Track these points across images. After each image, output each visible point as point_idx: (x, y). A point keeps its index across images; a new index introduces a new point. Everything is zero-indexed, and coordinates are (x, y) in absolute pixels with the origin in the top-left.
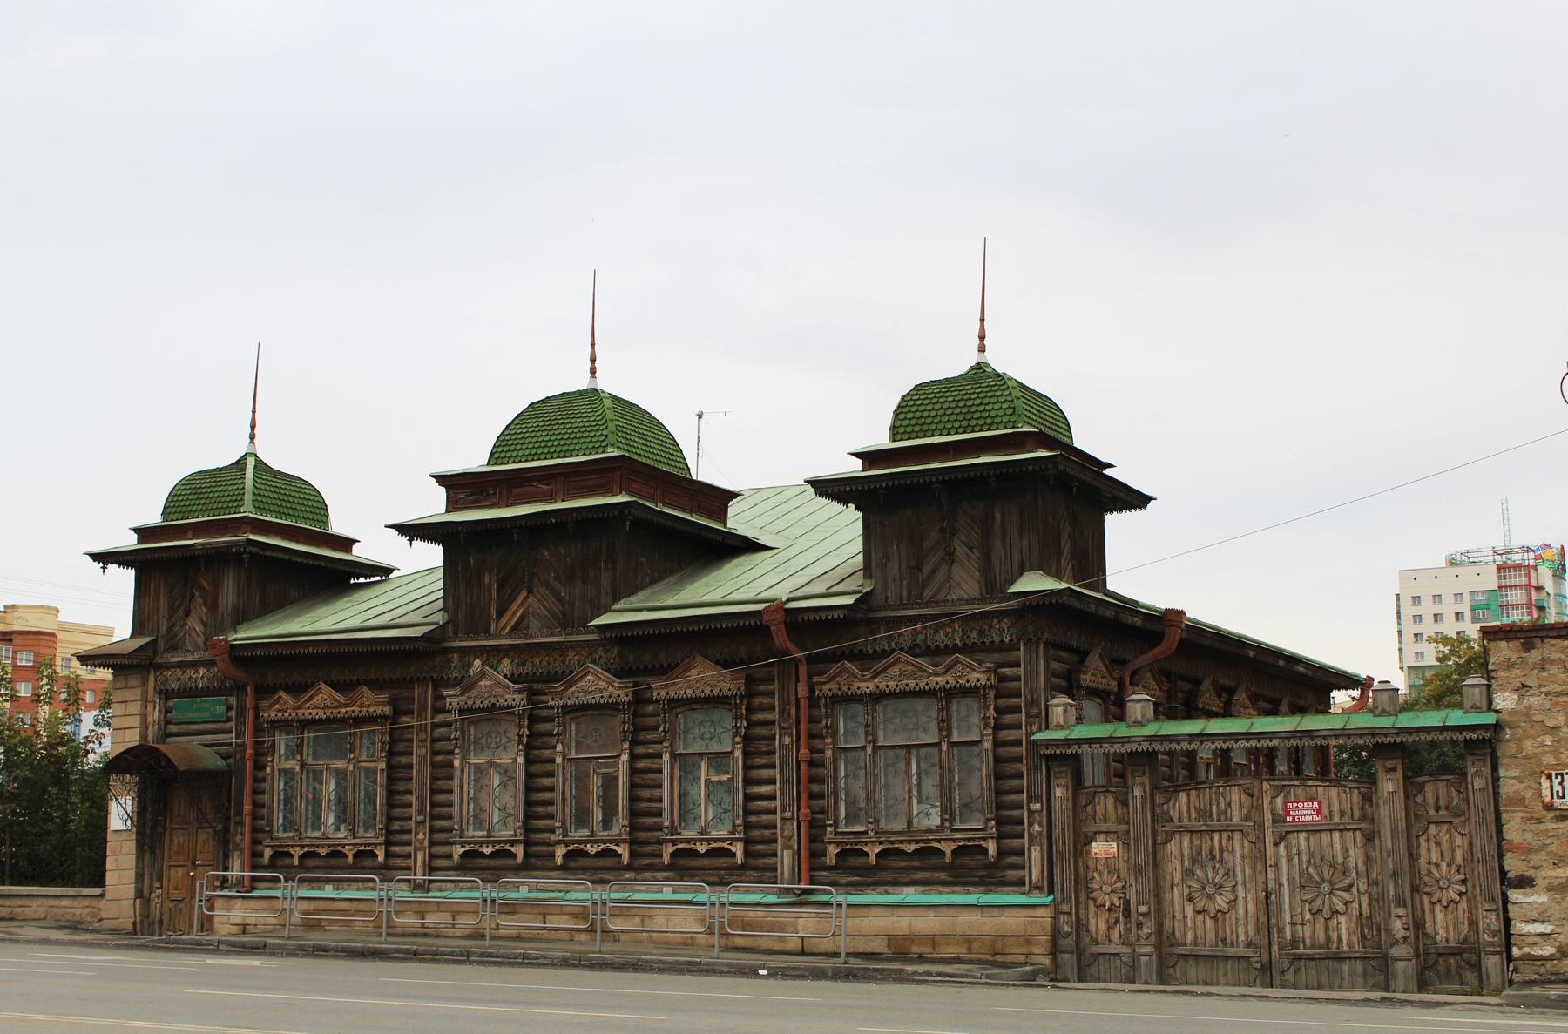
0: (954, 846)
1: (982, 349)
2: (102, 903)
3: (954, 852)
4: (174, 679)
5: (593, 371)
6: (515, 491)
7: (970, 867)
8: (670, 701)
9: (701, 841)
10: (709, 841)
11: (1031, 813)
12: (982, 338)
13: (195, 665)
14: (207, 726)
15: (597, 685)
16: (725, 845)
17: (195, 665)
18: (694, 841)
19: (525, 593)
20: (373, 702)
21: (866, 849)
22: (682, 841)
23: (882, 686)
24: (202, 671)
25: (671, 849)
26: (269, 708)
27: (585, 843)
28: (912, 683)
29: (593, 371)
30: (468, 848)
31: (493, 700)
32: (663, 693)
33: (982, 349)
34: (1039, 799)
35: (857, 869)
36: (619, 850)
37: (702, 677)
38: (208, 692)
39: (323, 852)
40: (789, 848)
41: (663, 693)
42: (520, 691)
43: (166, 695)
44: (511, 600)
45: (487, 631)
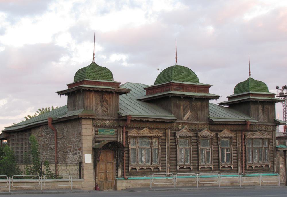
0: (265, 165)
1: (250, 75)
2: (83, 183)
3: (265, 167)
4: (99, 123)
5: (176, 61)
6: (187, 89)
7: (267, 170)
8: (221, 137)
9: (226, 165)
10: (227, 165)
11: (275, 160)
12: (250, 73)
13: (105, 120)
14: (110, 136)
15: (206, 132)
16: (230, 166)
17: (105, 120)
18: (225, 165)
19: (190, 112)
20: (161, 134)
21: (252, 166)
22: (223, 165)
23: (256, 137)
24: (108, 122)
25: (221, 167)
26: (131, 133)
27: (225, 165)
28: (260, 137)
29: (176, 61)
30: (181, 167)
31: (187, 135)
32: (220, 135)
33: (250, 75)
34: (276, 158)
35: (251, 170)
36: (211, 167)
37: (226, 133)
38: (109, 127)
39: (145, 168)
40: (240, 166)
41: (220, 135)
42: (192, 133)
43: (95, 127)
44: (187, 112)
45: (182, 119)
